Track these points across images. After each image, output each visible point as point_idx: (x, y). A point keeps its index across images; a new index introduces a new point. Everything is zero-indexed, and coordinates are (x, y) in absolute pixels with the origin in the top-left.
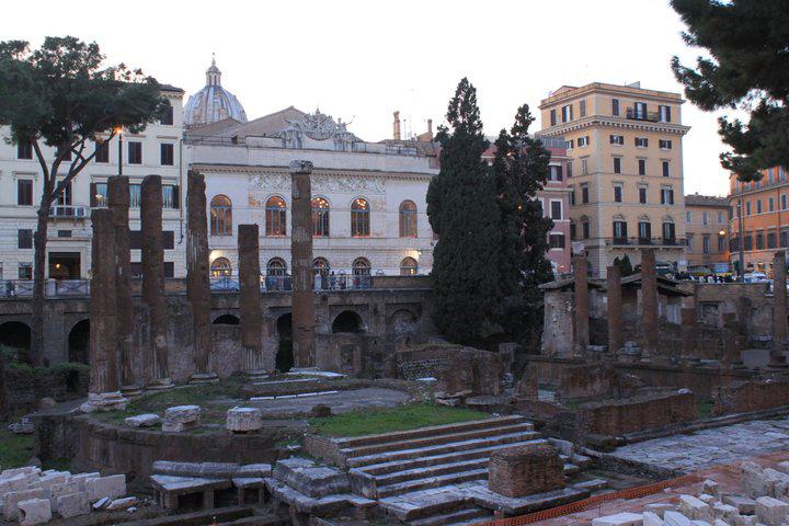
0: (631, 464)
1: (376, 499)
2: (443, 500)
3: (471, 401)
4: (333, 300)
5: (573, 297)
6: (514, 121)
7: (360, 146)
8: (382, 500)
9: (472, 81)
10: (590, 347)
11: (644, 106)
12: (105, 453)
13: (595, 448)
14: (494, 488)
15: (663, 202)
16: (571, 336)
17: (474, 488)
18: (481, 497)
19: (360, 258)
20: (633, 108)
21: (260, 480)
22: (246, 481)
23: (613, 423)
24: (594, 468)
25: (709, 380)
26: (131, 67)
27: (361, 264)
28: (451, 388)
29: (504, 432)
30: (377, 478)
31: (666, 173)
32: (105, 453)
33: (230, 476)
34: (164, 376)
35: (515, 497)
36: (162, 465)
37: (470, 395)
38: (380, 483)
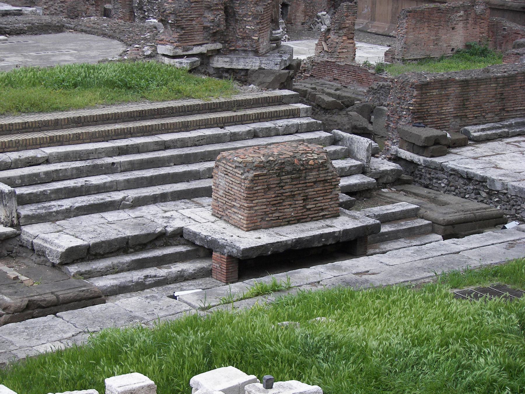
0: (469, 178)
1: (18, 226)
3: (220, 62)
8: (27, 229)
13: (413, 148)
14: (220, 214)
17: (187, 212)
18: (194, 228)
23: (450, 107)
24: (408, 182)
28: (185, 37)
29: (260, 118)
30: (19, 191)
35: (249, 229)
37: (218, 52)
38: (23, 200)
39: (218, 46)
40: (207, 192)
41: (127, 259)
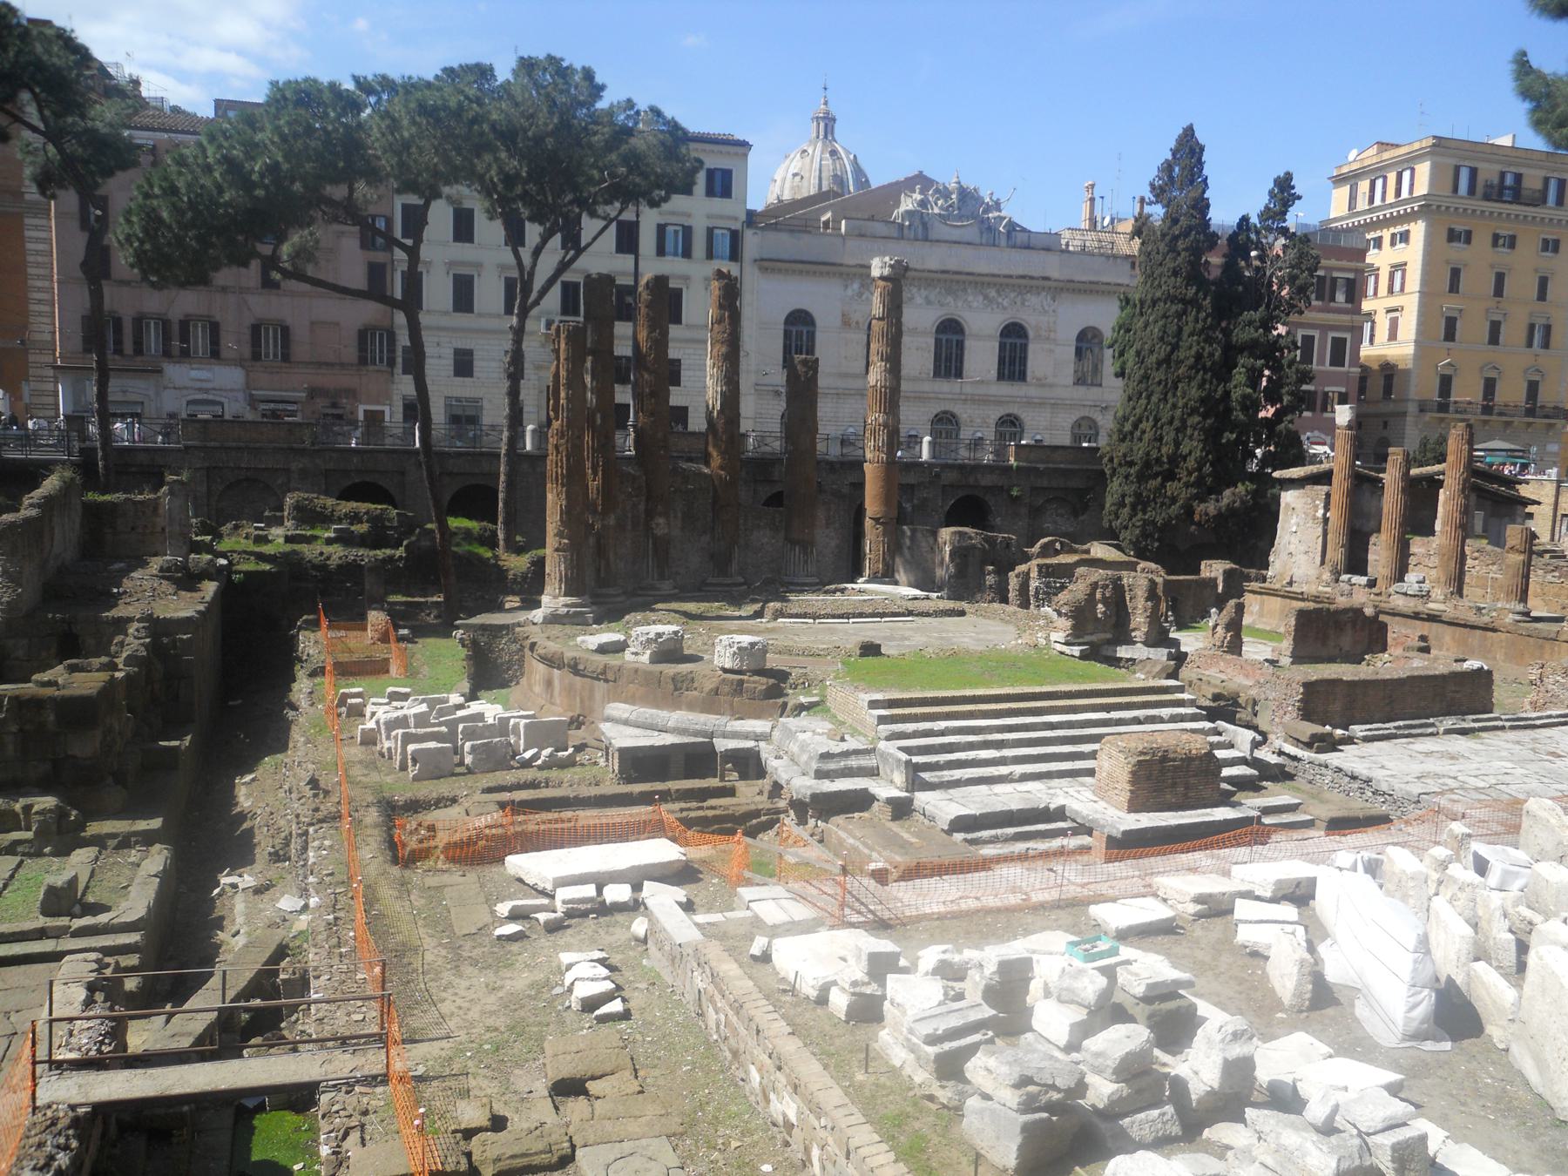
2: (1015, 806)
4: (950, 477)
5: (1328, 495)
6: (1266, 199)
7: (1020, 238)
9: (1201, 136)
10: (1345, 577)
11: (1518, 178)
12: (549, 683)
13: (1297, 742)
15: (1530, 344)
16: (1318, 559)
19: (945, 412)
20: (1496, 181)
21: (750, 744)
22: (732, 744)
25: (1542, 647)
26: (642, 105)
27: (1010, 425)
30: (915, 759)
31: (1542, 296)
32: (549, 683)
33: (712, 735)
34: (662, 577)
36: (619, 709)
39: (1109, 636)
40: (1091, 772)
41: (1011, 831)
